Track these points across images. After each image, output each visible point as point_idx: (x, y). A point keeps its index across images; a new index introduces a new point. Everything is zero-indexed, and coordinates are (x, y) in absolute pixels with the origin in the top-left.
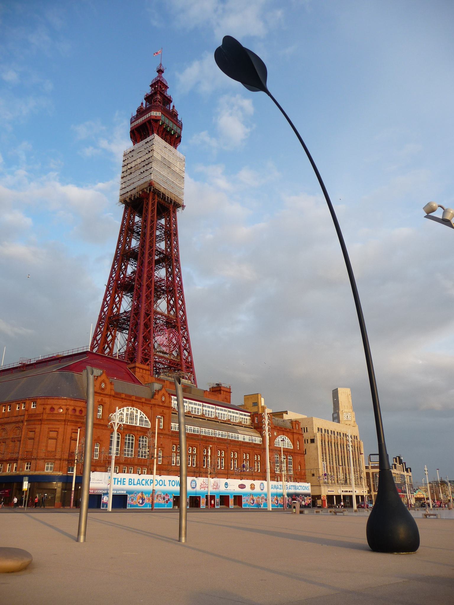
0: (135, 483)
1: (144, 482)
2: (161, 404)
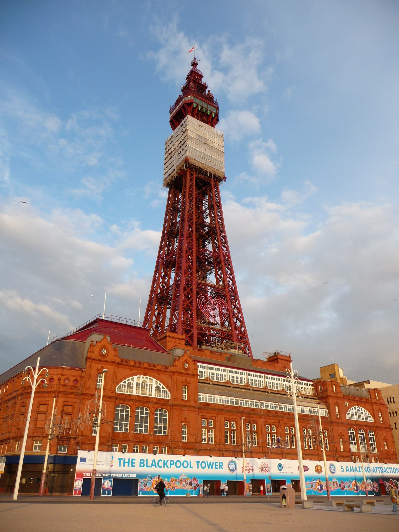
0: (149, 464)
1: (161, 464)
2: (183, 371)
